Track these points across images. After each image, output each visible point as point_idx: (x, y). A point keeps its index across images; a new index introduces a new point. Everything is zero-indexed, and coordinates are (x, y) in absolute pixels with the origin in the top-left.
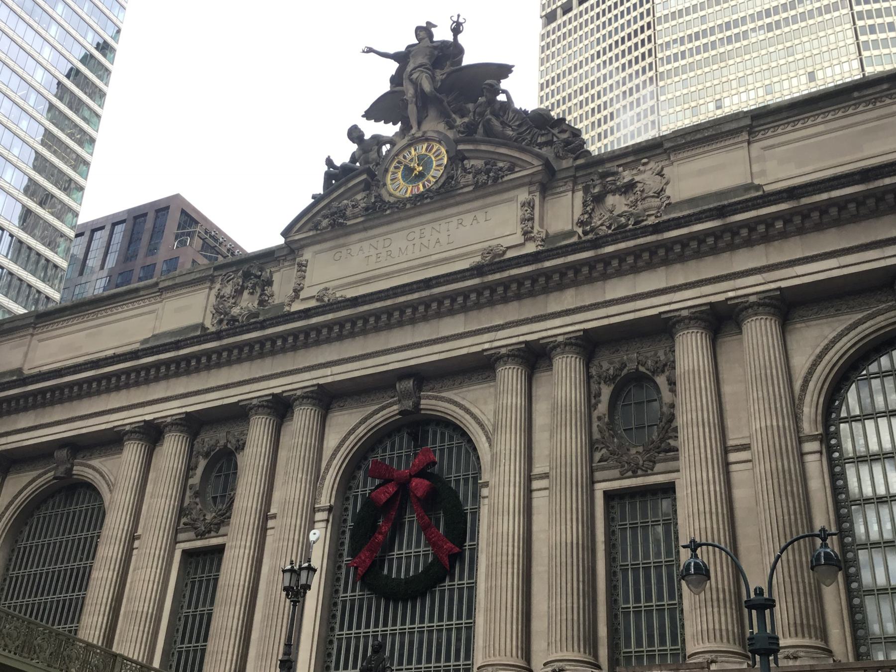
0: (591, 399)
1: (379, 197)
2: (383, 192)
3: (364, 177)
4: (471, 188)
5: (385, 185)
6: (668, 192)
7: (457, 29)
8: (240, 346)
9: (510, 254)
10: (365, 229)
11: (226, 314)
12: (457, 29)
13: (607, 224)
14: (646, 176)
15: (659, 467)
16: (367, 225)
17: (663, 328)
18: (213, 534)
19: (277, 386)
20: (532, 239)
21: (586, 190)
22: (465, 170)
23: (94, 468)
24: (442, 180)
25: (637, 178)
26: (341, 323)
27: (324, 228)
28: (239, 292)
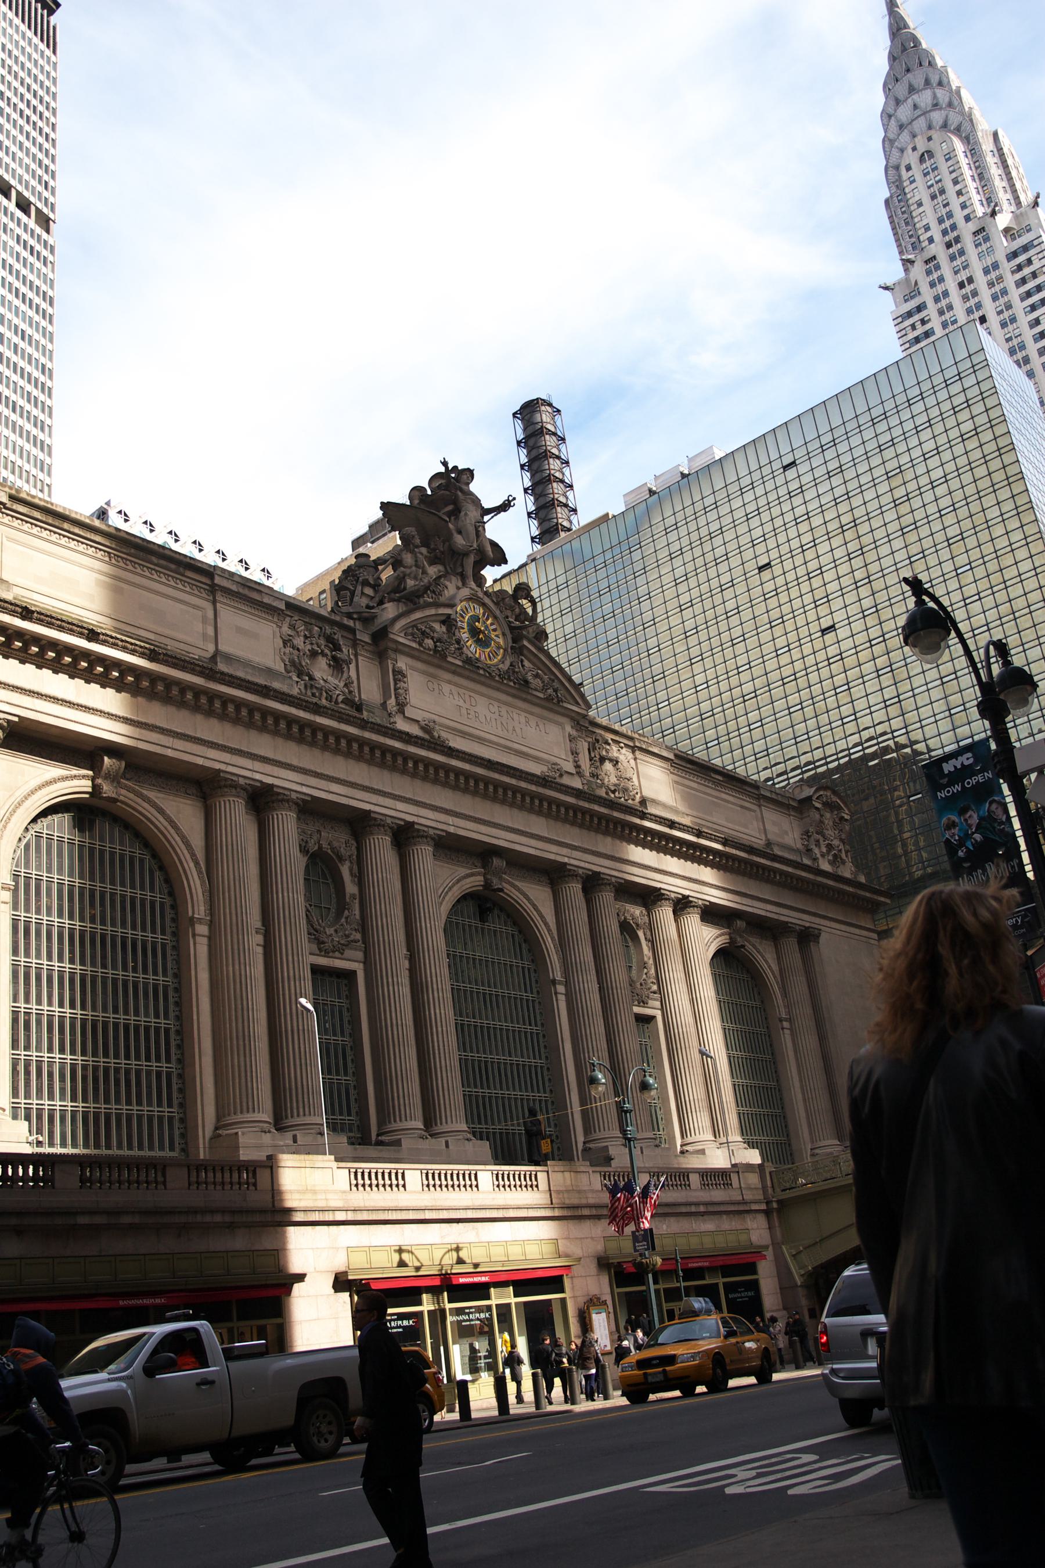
1: (458, 642)
4: (541, 695)
9: (566, 780)
10: (454, 673)
11: (311, 678)
13: (613, 788)
16: (458, 670)
18: (337, 954)
19: (405, 812)
20: (580, 774)
22: (523, 666)
24: (508, 663)
25: (622, 758)
26: (468, 776)
27: (430, 649)
28: (314, 654)
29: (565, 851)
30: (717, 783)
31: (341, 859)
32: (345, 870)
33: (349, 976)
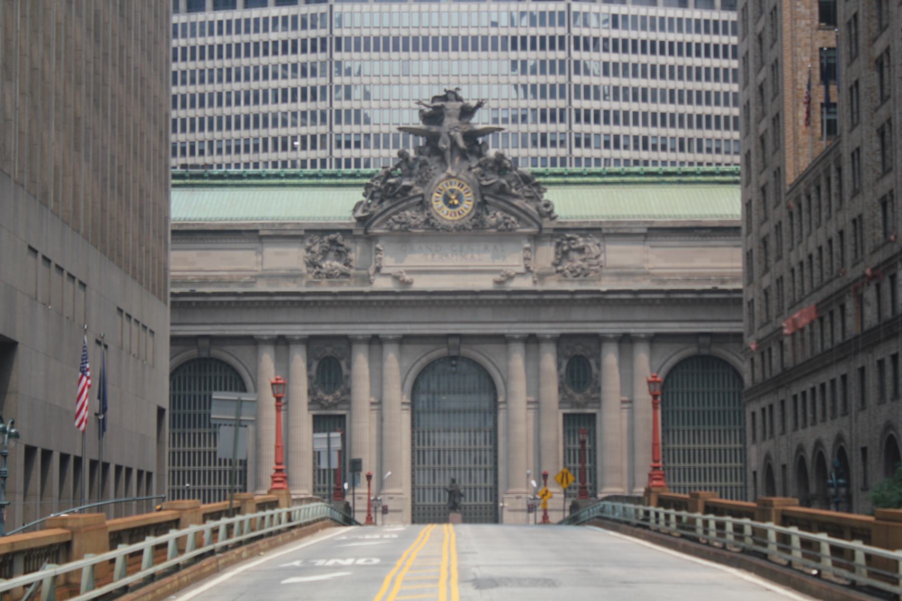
0: (559, 366)
2: (431, 210)
3: (420, 199)
5: (432, 205)
6: (602, 258)
7: (480, 105)
8: (347, 302)
11: (321, 267)
12: (480, 105)
14: (592, 245)
15: (590, 405)
17: (599, 340)
21: (558, 245)
23: (229, 353)
24: (473, 214)
28: (325, 254)
29: (506, 326)
30: (705, 236)
31: (342, 358)
32: (343, 364)
33: (343, 417)
